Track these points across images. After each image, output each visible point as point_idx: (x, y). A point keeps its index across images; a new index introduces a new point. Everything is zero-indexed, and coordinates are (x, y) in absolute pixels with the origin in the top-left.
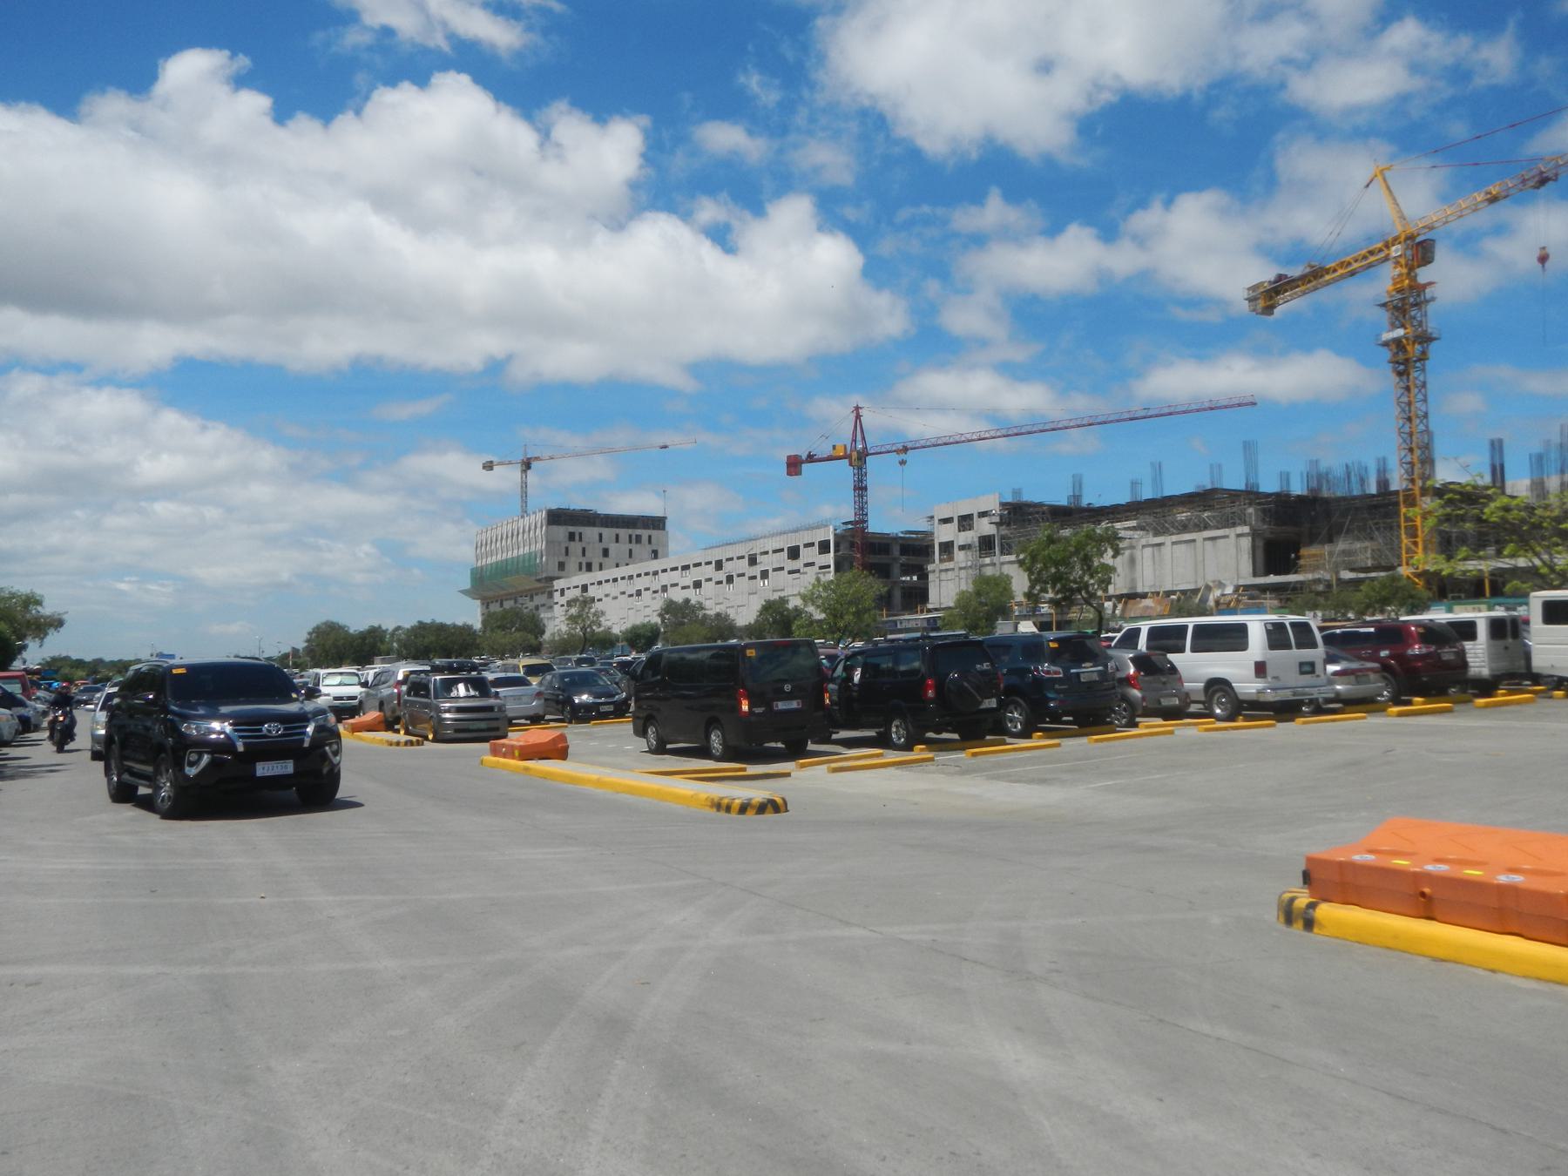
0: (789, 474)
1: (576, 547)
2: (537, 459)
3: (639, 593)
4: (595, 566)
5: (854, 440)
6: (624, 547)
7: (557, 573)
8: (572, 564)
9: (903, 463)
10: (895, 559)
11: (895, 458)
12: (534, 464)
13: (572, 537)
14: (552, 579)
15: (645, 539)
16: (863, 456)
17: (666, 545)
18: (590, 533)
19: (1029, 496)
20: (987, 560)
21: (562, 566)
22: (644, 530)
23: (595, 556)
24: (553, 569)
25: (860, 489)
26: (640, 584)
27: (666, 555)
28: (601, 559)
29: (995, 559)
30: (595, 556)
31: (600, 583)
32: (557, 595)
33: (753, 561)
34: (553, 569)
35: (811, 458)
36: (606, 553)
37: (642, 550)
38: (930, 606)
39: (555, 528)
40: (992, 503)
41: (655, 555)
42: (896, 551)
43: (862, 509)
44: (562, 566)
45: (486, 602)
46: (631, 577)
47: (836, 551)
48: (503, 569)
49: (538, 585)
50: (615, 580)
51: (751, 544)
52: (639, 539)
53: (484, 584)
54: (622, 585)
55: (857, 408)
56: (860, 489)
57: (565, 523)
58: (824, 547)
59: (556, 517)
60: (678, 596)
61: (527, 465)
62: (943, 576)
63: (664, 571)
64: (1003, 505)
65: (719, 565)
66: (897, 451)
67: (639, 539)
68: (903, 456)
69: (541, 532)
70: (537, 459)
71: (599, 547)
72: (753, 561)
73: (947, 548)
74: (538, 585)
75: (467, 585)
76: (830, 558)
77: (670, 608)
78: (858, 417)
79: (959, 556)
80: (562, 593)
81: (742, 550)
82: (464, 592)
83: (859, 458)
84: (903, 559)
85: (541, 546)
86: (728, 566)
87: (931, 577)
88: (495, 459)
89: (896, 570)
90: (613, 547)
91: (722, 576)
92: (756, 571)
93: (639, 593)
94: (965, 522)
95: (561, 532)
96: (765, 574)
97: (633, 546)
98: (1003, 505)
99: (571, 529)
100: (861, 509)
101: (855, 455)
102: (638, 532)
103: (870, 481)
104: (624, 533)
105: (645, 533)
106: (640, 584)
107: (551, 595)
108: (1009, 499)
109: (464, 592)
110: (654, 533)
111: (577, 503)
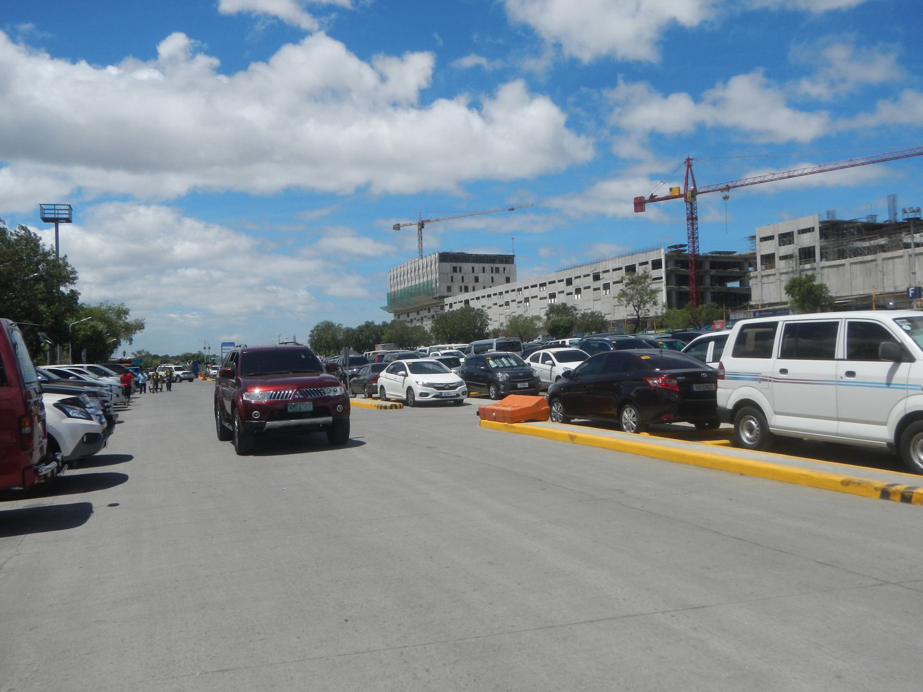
0: (636, 211)
1: (458, 276)
2: (428, 221)
3: (507, 304)
4: (470, 288)
5: (686, 184)
6: (488, 275)
8: (455, 288)
9: (726, 198)
10: (706, 272)
11: (719, 195)
12: (426, 225)
13: (455, 270)
14: (444, 297)
15: (501, 270)
16: (694, 193)
17: (515, 274)
18: (467, 267)
19: (843, 215)
20: (808, 266)
21: (449, 289)
22: (500, 263)
23: (470, 282)
24: (444, 291)
25: (692, 219)
26: (508, 297)
27: (515, 280)
28: (474, 284)
29: (815, 265)
30: (470, 282)
31: (478, 298)
33: (597, 277)
34: (444, 291)
35: (653, 199)
36: (477, 280)
37: (499, 277)
38: (752, 303)
40: (813, 221)
41: (508, 280)
42: (707, 266)
43: (693, 233)
44: (449, 289)
45: (398, 314)
46: (501, 293)
47: (666, 267)
48: (410, 293)
49: (435, 301)
50: (489, 296)
51: (595, 266)
52: (497, 270)
53: (396, 302)
54: (494, 299)
55: (688, 160)
56: (692, 219)
58: (657, 264)
59: (444, 257)
60: (559, 300)
61: (421, 225)
62: (765, 280)
63: (526, 288)
64: (821, 222)
65: (569, 282)
66: (722, 190)
67: (497, 270)
68: (726, 193)
69: (435, 267)
70: (428, 221)
71: (473, 276)
72: (597, 277)
73: (769, 260)
74: (435, 301)
75: (385, 304)
76: (662, 272)
77: (553, 309)
78: (689, 166)
79: (781, 265)
81: (589, 270)
82: (382, 308)
83: (691, 197)
84: (713, 272)
85: (435, 276)
86: (576, 283)
87: (751, 282)
88: (401, 223)
89: (708, 280)
90: (481, 276)
91: (571, 289)
92: (599, 284)
93: (507, 304)
94: (786, 238)
95: (448, 266)
96: (607, 286)
97: (494, 275)
98: (821, 222)
99: (454, 264)
100: (693, 236)
101: (689, 194)
102: (497, 265)
103: (700, 214)
104: (488, 266)
105: (501, 266)
106: (508, 297)
107: (442, 308)
108: (825, 219)
109: (382, 308)
110: (507, 266)
111: (456, 249)
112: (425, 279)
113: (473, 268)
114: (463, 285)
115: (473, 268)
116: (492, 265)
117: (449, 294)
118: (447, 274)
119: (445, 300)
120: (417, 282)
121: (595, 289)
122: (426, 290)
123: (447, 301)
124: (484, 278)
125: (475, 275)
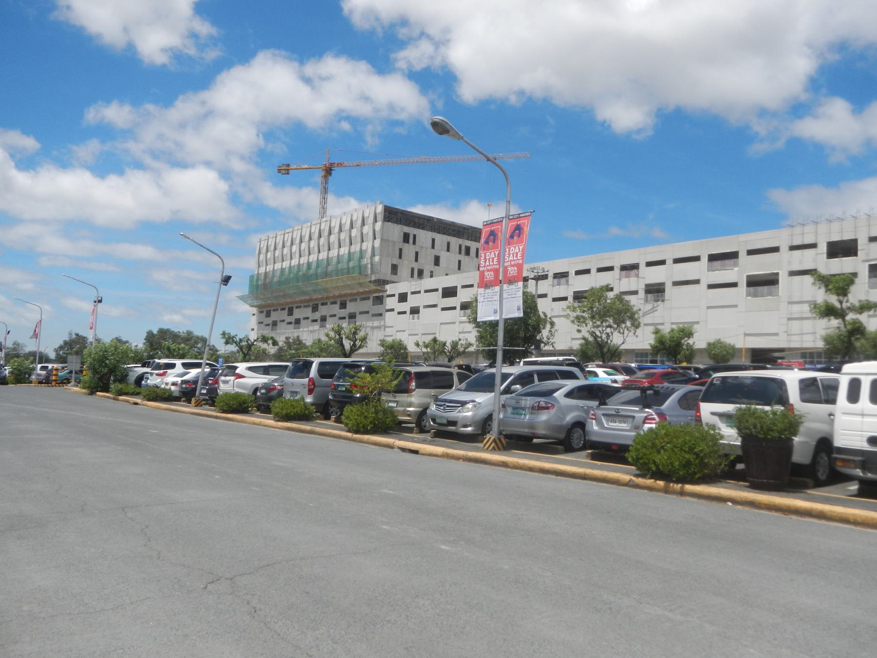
1: (409, 250)
2: (340, 165)
4: (426, 273)
7: (389, 277)
13: (406, 238)
14: (386, 282)
15: (473, 252)
18: (424, 236)
21: (394, 268)
24: (385, 272)
32: (391, 303)
34: (385, 272)
39: (386, 223)
44: (394, 268)
52: (468, 251)
57: (398, 221)
59: (392, 215)
70: (340, 165)
80: (403, 298)
90: (444, 256)
95: (396, 231)
97: (462, 257)
99: (407, 229)
102: (468, 243)
104: (455, 242)
107: (379, 300)
112: (344, 251)
113: (433, 240)
114: (416, 266)
115: (433, 240)
116: (460, 241)
117: (394, 278)
118: (394, 243)
119: (388, 287)
120: (323, 255)
121: (399, 313)
122: (354, 267)
123: (390, 289)
124: (449, 259)
125: (435, 252)
